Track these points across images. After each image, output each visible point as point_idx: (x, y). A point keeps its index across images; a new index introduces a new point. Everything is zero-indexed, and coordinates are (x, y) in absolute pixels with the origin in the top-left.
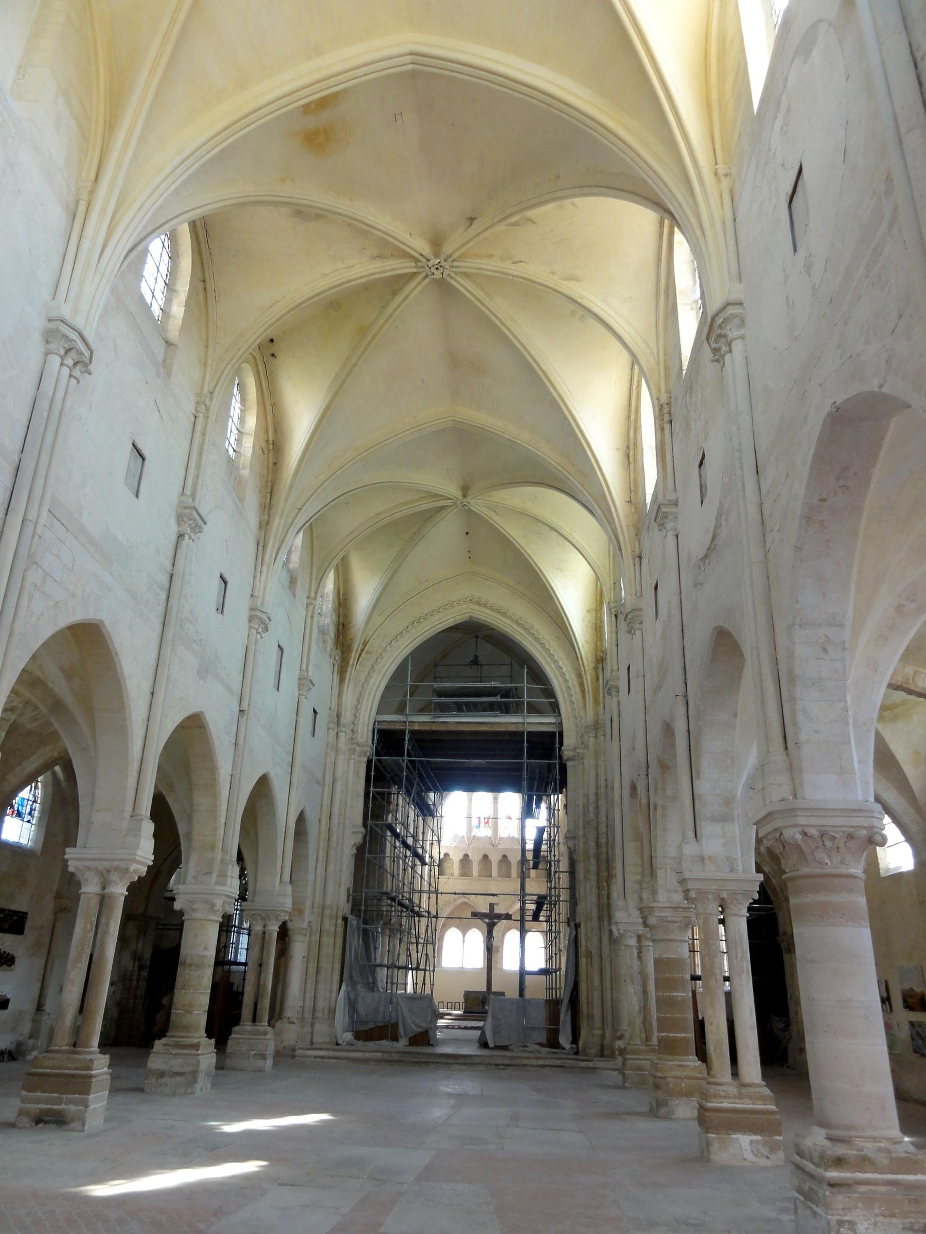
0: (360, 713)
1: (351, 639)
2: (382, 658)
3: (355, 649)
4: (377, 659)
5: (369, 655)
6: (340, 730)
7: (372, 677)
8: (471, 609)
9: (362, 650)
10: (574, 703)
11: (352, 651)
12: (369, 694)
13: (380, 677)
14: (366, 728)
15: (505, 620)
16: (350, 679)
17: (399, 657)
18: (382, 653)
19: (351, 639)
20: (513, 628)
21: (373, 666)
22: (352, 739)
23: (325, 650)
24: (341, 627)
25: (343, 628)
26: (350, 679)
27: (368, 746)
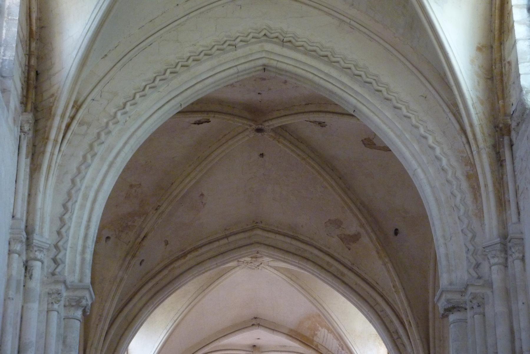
0: (69, 228)
1: (53, 95)
2: (109, 132)
3: (59, 112)
4: (99, 135)
5: (85, 128)
6: (32, 255)
7: (89, 166)
8: (267, 51)
9: (72, 118)
10: (459, 210)
11: (54, 116)
12: (85, 197)
13: (105, 168)
14: (78, 258)
15: (326, 69)
16: (49, 166)
17: (139, 133)
18: (107, 124)
19: (53, 95)
20: (343, 83)
21: (91, 147)
22: (53, 274)
23: (7, 104)
24: (33, 74)
25: (37, 79)
26: (49, 166)
27: (84, 288)
